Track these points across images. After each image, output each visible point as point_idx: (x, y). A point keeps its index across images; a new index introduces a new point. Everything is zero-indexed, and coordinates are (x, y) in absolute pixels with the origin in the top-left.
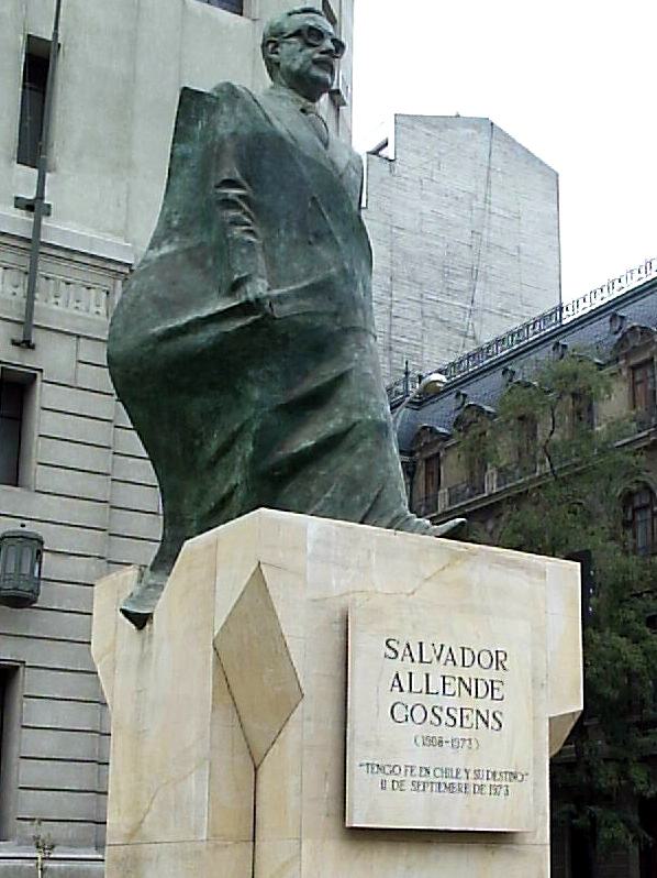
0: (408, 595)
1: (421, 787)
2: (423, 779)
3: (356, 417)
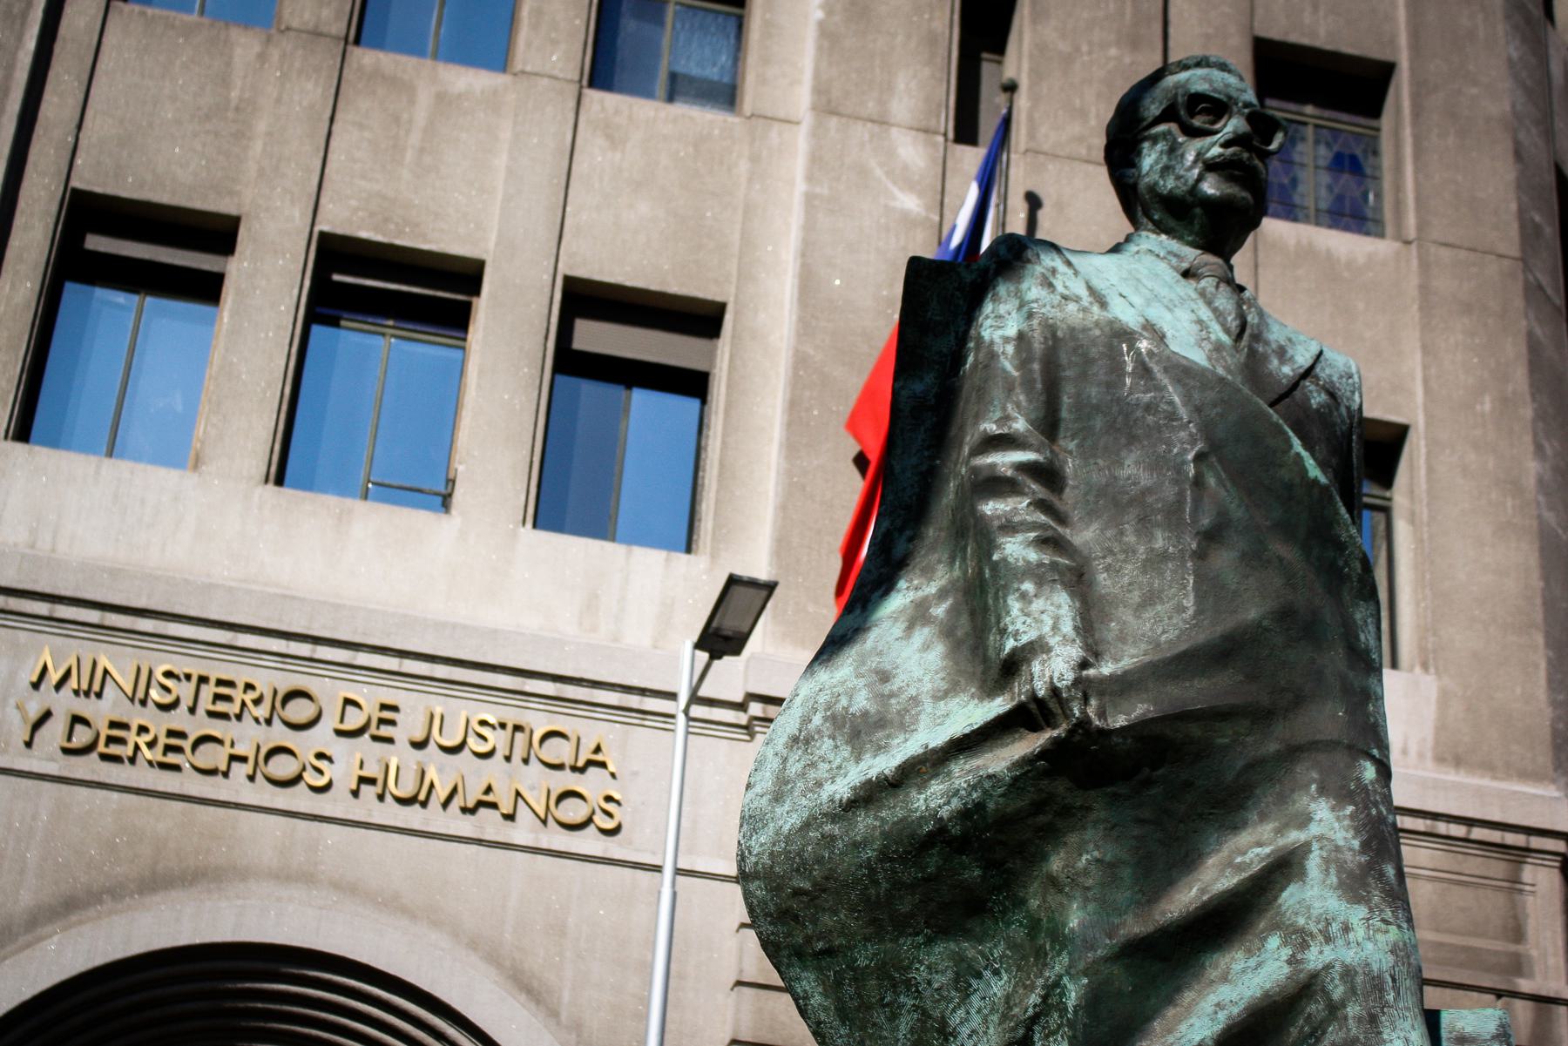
3: (1315, 957)
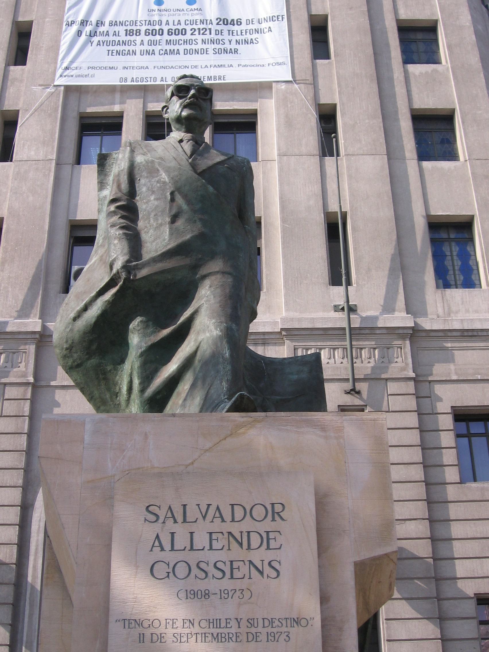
0: (187, 466)
1: (184, 639)
2: (187, 631)
3: (201, 337)
